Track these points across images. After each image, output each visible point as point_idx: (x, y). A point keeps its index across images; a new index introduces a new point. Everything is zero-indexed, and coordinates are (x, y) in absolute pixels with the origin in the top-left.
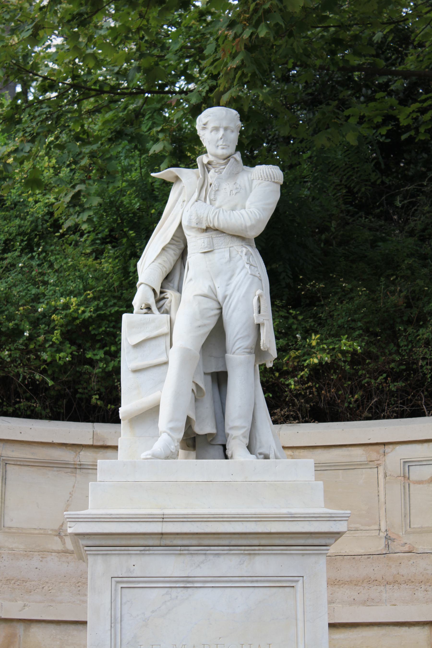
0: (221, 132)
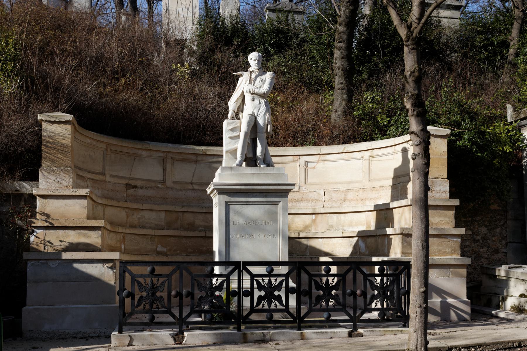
0: (257, 61)
